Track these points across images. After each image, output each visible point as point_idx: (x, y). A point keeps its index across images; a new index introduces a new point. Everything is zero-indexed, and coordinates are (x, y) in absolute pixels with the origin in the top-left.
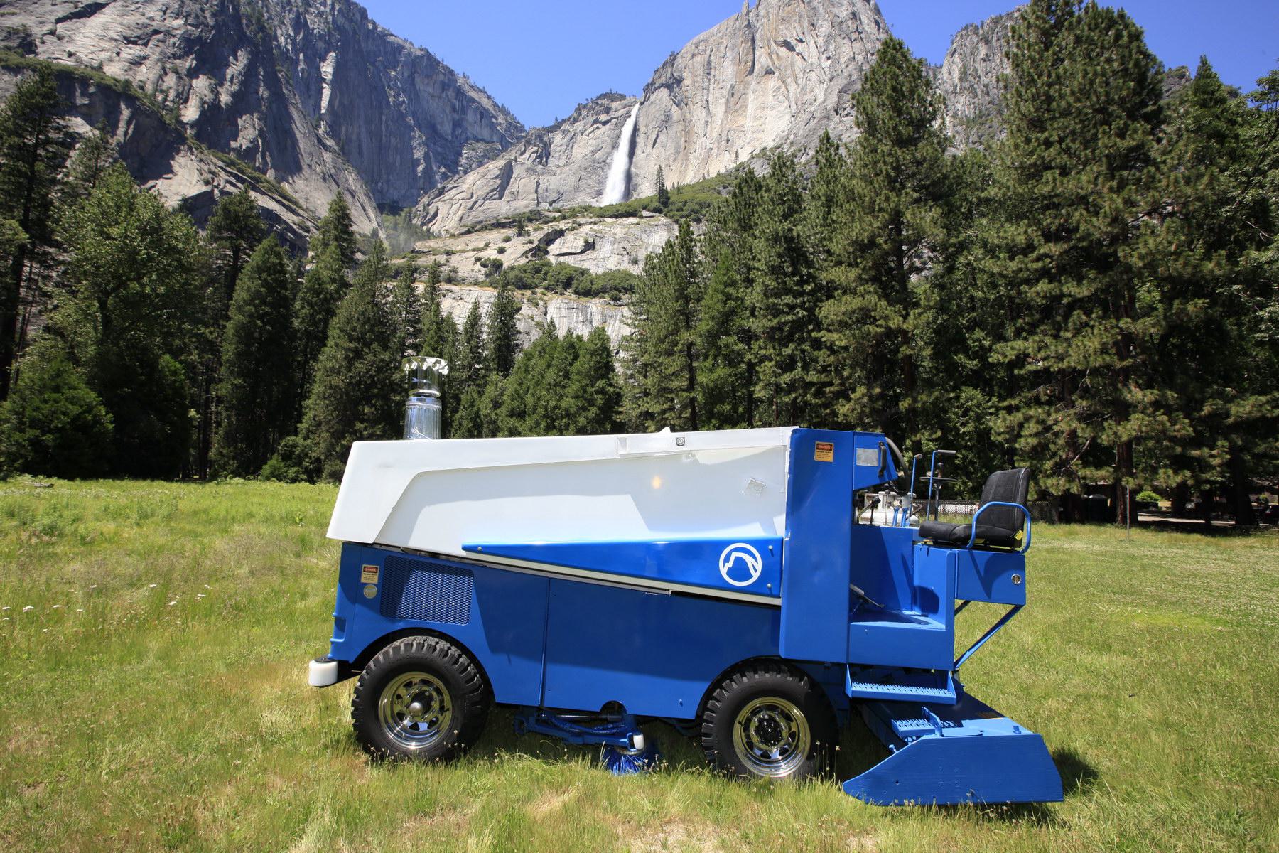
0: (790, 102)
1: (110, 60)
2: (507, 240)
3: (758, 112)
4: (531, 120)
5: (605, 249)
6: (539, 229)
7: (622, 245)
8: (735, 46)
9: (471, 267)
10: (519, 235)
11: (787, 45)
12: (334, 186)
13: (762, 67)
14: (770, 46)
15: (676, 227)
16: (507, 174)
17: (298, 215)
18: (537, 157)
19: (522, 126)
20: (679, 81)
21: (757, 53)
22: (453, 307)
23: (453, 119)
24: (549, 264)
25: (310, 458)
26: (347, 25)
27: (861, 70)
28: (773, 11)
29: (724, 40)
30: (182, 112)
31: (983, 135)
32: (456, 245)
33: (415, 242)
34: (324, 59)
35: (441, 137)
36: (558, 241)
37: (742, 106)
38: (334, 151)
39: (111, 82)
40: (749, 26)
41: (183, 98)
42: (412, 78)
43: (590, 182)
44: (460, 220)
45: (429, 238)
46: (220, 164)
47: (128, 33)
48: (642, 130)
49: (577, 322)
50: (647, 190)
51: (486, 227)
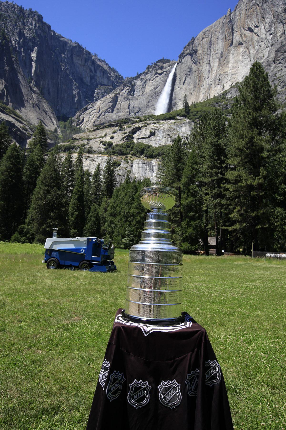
0: (250, 58)
2: (115, 132)
3: (235, 64)
6: (129, 127)
7: (167, 133)
8: (223, 32)
9: (98, 146)
10: (120, 130)
12: (38, 109)
13: (237, 41)
14: (241, 30)
15: (193, 124)
16: (115, 100)
18: (129, 92)
19: (122, 77)
20: (196, 52)
21: (235, 35)
22: (90, 164)
23: (91, 75)
24: (133, 143)
25: (30, 233)
28: (243, 12)
29: (218, 30)
33: (74, 134)
34: (32, 51)
36: (138, 132)
38: (37, 93)
40: (231, 21)
43: (153, 102)
44: (94, 123)
45: (80, 133)
48: (178, 76)
49: (146, 170)
50: (180, 106)
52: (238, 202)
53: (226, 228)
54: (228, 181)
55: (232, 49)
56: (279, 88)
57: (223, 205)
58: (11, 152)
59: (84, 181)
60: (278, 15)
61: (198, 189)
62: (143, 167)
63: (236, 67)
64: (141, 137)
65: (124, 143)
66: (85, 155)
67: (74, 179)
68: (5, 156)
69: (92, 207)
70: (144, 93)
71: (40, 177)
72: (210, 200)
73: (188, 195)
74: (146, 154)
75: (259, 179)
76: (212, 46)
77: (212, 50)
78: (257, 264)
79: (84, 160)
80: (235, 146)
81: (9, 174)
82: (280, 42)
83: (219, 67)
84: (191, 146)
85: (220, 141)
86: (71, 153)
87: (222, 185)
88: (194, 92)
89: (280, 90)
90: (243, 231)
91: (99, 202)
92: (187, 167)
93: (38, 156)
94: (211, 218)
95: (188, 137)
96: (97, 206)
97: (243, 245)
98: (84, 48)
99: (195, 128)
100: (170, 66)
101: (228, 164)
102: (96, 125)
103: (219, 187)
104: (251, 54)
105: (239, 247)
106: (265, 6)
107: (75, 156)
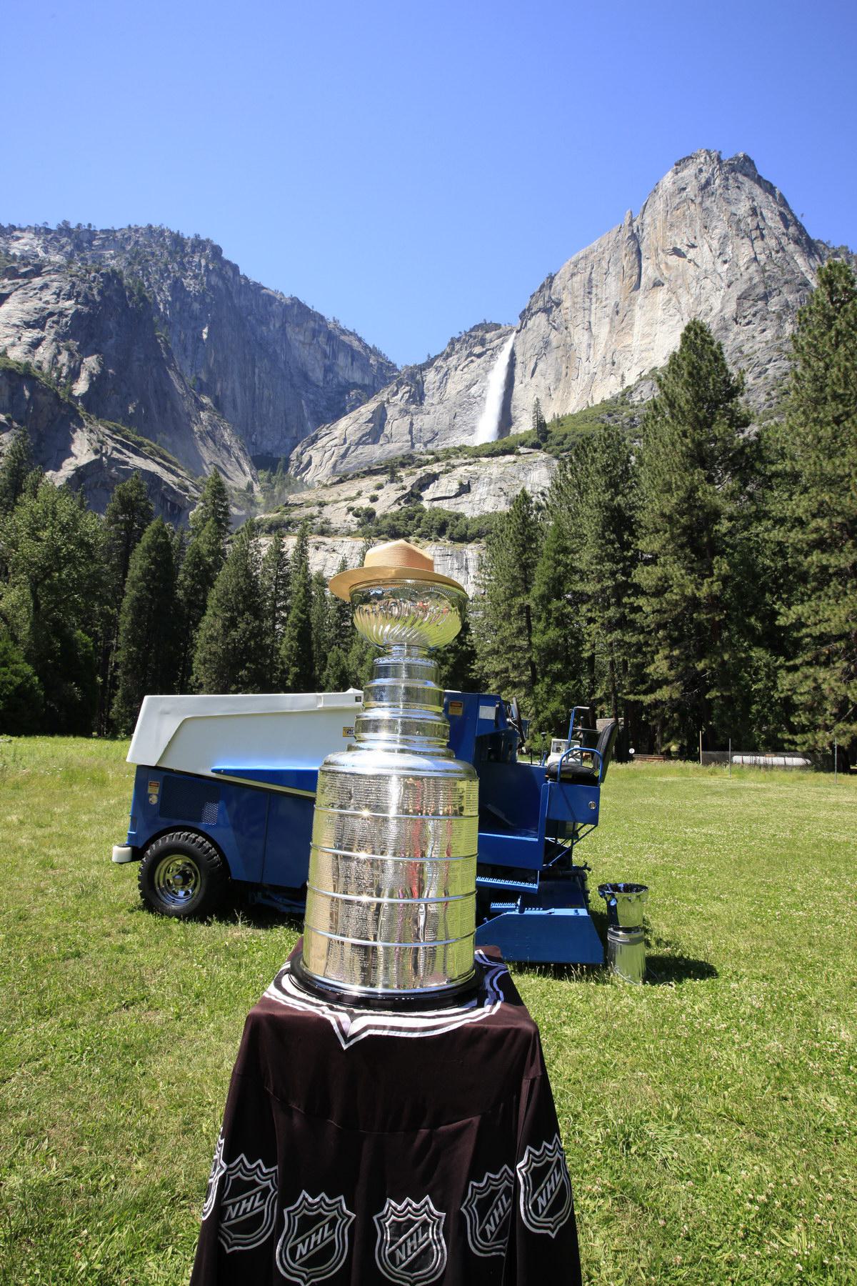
0: (682, 314)
1: (13, 345)
2: (380, 487)
4: (403, 357)
5: (480, 491)
6: (412, 474)
7: (498, 485)
10: (392, 481)
11: (677, 252)
12: (210, 443)
13: (649, 279)
14: (657, 255)
15: (556, 462)
16: (379, 418)
17: (178, 476)
18: (410, 397)
19: (394, 366)
20: (558, 304)
21: (644, 265)
22: (325, 560)
24: (422, 510)
26: (220, 284)
27: (764, 271)
28: (661, 217)
29: (607, 256)
30: (74, 386)
32: (328, 495)
33: (289, 493)
35: (312, 384)
36: (432, 486)
38: (210, 409)
39: (14, 366)
40: (634, 237)
41: (74, 375)
44: (334, 466)
46: (107, 432)
47: (27, 318)
48: (519, 359)
49: (452, 569)
50: (524, 424)
51: (358, 475)
52: (665, 638)
53: (637, 698)
54: (638, 590)
55: (640, 296)
56: (749, 379)
57: (630, 645)
59: (311, 597)
60: (740, 220)
61: (569, 609)
64: (437, 496)
66: (313, 539)
67: (290, 593)
68: (140, 548)
69: (329, 655)
72: (598, 633)
73: (549, 624)
74: (451, 534)
75: (712, 582)
77: (594, 300)
78: (712, 781)
79: (311, 551)
80: (653, 510)
81: (148, 585)
82: (746, 277)
84: (551, 512)
85: (619, 498)
86: (283, 536)
87: (625, 600)
90: (676, 706)
91: (346, 643)
92: (544, 559)
93: (210, 544)
94: (602, 674)
95: (547, 492)
96: (341, 653)
97: (679, 737)
99: (561, 471)
102: (340, 472)
103: (619, 604)
104: (683, 306)
105: (668, 741)
106: (707, 203)
107: (291, 542)
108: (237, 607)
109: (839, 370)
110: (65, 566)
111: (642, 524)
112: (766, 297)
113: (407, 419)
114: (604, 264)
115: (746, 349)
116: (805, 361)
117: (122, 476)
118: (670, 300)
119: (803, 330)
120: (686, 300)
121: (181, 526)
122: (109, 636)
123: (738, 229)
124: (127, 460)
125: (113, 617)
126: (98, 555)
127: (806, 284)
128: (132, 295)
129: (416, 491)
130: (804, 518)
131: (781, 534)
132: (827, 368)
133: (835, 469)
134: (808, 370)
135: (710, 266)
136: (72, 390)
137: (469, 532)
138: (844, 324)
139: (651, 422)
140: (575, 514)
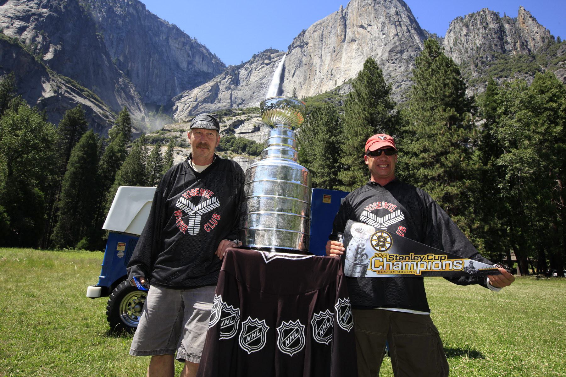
3: (348, 60)
4: (229, 60)
5: (264, 130)
6: (230, 119)
11: (362, 27)
12: (123, 94)
13: (350, 38)
16: (215, 91)
17: (103, 109)
19: (224, 65)
20: (307, 44)
21: (347, 31)
24: (235, 138)
26: (135, 13)
27: (401, 40)
28: (356, 10)
29: (330, 24)
31: (465, 74)
36: (240, 126)
37: (339, 57)
42: (167, 39)
43: (258, 94)
46: (63, 82)
48: (287, 68)
54: (341, 183)
55: (345, 45)
56: (394, 88)
58: (86, 140)
60: (391, 16)
62: (245, 165)
63: (349, 63)
64: (243, 131)
65: (224, 137)
66: (176, 149)
68: (78, 145)
70: (249, 83)
71: (120, 171)
74: (249, 151)
76: (324, 39)
79: (175, 155)
80: (349, 144)
82: (393, 42)
83: (331, 62)
84: (300, 142)
85: (333, 137)
86: (160, 146)
87: (334, 187)
88: (304, 85)
89: (395, 90)
93: (119, 146)
98: (182, 29)
100: (277, 57)
101: (341, 163)
104: (364, 52)
106: (377, 7)
107: (164, 150)
108: (133, 181)
109: (433, 87)
110: (31, 152)
111: (344, 151)
112: (401, 52)
113: (229, 92)
114: (329, 28)
115: (392, 74)
116: (418, 80)
117: (69, 106)
118: (359, 48)
119: (418, 68)
120: (366, 49)
121: (103, 136)
122: (53, 194)
123: (390, 20)
124: (74, 98)
125: (59, 181)
126: (53, 147)
127: (419, 48)
128: (84, 11)
129: (232, 128)
130: (417, 152)
131: (407, 159)
132: (428, 85)
133: (431, 130)
134: (420, 85)
135: (377, 35)
136: (43, 57)
137: (258, 151)
138: (435, 66)
139: (349, 103)
140: (312, 144)
